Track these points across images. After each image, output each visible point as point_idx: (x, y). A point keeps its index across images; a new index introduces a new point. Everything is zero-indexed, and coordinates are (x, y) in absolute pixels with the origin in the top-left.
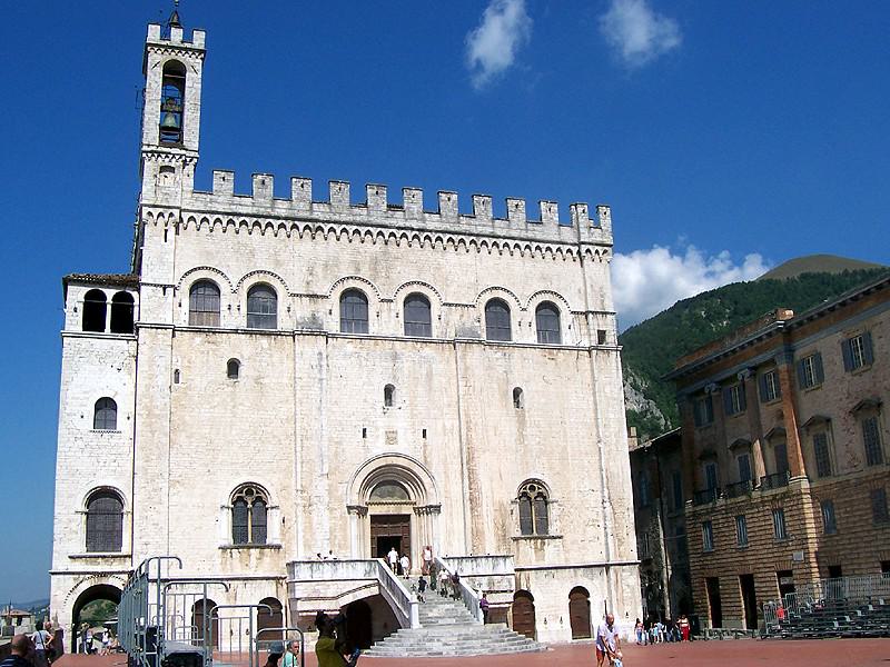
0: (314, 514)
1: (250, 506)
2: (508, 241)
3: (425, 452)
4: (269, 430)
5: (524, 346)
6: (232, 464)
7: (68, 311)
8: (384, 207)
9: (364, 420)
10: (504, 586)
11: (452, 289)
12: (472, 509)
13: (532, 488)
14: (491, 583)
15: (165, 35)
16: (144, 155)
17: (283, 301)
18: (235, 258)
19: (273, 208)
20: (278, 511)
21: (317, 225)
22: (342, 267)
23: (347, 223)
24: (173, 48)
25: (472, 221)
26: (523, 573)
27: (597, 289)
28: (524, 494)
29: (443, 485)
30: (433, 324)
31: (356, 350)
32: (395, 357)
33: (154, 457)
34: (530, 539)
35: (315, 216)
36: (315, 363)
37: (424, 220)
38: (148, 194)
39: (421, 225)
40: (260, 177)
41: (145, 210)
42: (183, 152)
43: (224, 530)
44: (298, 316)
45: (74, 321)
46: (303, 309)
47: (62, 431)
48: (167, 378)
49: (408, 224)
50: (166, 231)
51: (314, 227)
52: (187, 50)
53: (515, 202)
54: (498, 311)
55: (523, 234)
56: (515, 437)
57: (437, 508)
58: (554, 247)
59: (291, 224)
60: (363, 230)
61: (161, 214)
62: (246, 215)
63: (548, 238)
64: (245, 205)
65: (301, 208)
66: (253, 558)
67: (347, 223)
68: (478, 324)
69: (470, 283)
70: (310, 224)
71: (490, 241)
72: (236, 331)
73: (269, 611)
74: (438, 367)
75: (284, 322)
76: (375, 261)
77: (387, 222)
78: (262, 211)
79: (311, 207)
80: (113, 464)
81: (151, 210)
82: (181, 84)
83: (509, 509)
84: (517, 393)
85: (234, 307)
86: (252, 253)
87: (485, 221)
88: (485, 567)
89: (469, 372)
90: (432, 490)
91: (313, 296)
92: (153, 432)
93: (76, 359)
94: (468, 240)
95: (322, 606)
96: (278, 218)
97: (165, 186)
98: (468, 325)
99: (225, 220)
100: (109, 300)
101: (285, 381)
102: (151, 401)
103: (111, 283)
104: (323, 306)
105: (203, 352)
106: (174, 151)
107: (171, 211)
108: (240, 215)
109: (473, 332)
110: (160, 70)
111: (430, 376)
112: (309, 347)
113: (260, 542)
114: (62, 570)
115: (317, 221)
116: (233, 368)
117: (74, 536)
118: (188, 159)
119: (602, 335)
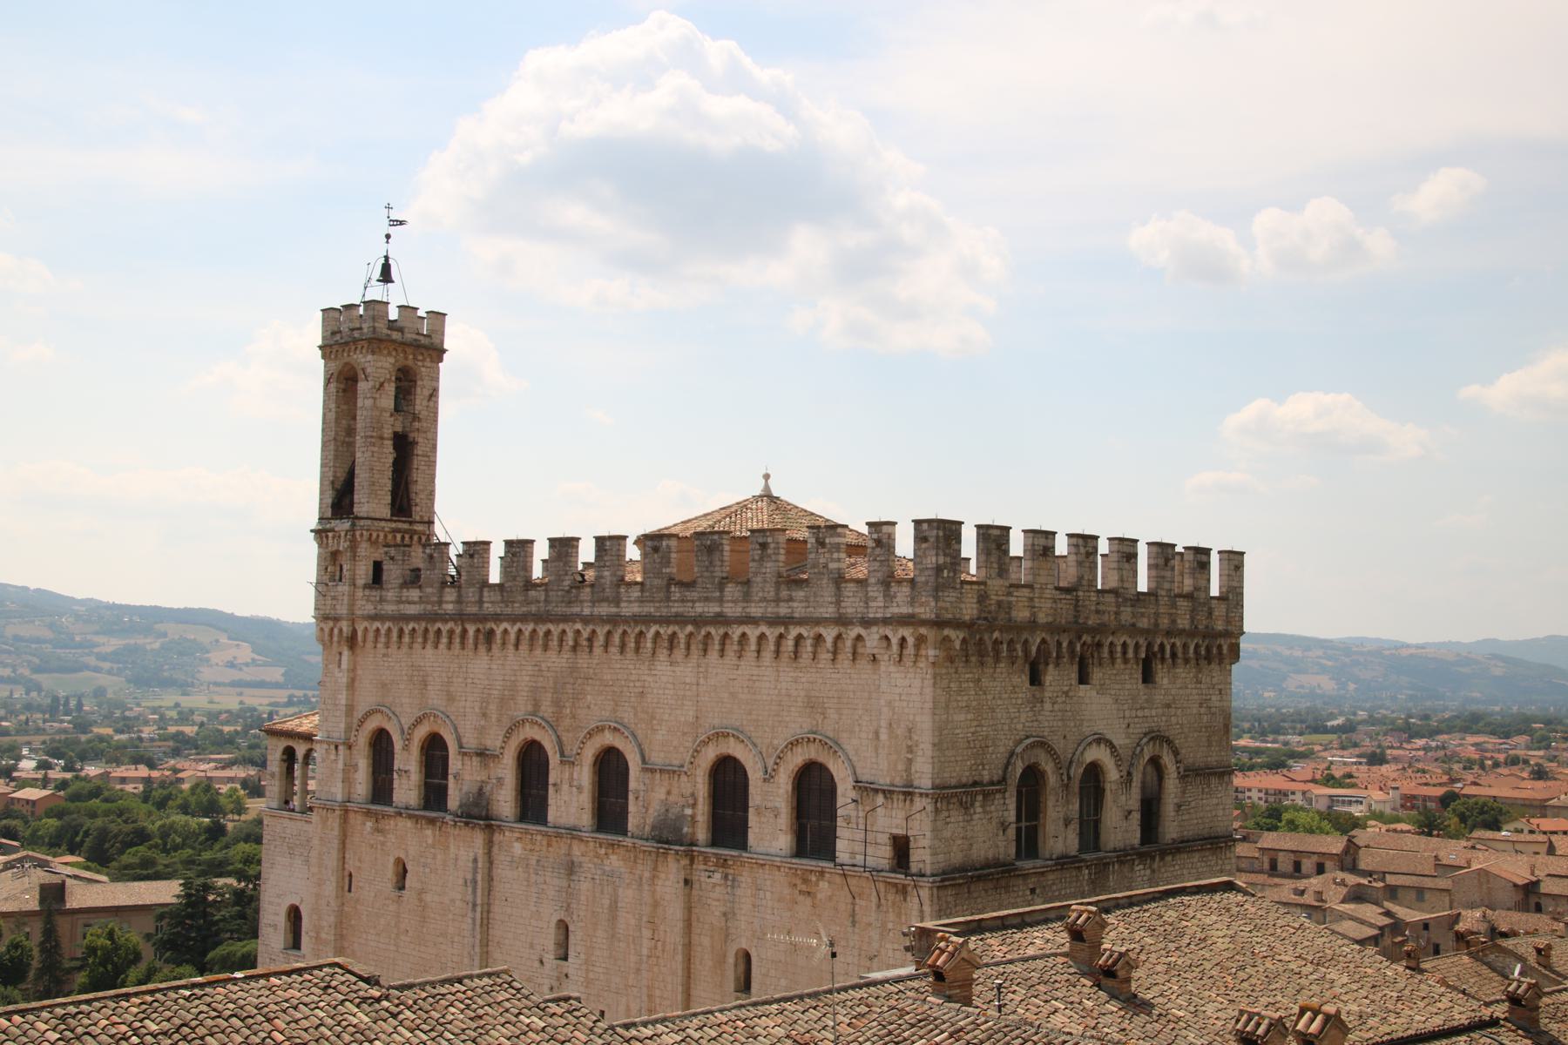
2: (748, 630)
11: (659, 737)
17: (454, 764)
19: (440, 603)
21: (489, 625)
32: (571, 869)
36: (469, 876)
37: (617, 601)
39: (614, 610)
44: (465, 789)
48: (330, 889)
49: (596, 611)
54: (728, 783)
55: (771, 610)
58: (829, 634)
62: (416, 618)
68: (688, 811)
71: (716, 632)
74: (627, 895)
77: (569, 611)
79: (481, 596)
86: (425, 684)
91: (483, 754)
111: (614, 907)
115: (482, 619)
116: (402, 873)
119: (901, 848)
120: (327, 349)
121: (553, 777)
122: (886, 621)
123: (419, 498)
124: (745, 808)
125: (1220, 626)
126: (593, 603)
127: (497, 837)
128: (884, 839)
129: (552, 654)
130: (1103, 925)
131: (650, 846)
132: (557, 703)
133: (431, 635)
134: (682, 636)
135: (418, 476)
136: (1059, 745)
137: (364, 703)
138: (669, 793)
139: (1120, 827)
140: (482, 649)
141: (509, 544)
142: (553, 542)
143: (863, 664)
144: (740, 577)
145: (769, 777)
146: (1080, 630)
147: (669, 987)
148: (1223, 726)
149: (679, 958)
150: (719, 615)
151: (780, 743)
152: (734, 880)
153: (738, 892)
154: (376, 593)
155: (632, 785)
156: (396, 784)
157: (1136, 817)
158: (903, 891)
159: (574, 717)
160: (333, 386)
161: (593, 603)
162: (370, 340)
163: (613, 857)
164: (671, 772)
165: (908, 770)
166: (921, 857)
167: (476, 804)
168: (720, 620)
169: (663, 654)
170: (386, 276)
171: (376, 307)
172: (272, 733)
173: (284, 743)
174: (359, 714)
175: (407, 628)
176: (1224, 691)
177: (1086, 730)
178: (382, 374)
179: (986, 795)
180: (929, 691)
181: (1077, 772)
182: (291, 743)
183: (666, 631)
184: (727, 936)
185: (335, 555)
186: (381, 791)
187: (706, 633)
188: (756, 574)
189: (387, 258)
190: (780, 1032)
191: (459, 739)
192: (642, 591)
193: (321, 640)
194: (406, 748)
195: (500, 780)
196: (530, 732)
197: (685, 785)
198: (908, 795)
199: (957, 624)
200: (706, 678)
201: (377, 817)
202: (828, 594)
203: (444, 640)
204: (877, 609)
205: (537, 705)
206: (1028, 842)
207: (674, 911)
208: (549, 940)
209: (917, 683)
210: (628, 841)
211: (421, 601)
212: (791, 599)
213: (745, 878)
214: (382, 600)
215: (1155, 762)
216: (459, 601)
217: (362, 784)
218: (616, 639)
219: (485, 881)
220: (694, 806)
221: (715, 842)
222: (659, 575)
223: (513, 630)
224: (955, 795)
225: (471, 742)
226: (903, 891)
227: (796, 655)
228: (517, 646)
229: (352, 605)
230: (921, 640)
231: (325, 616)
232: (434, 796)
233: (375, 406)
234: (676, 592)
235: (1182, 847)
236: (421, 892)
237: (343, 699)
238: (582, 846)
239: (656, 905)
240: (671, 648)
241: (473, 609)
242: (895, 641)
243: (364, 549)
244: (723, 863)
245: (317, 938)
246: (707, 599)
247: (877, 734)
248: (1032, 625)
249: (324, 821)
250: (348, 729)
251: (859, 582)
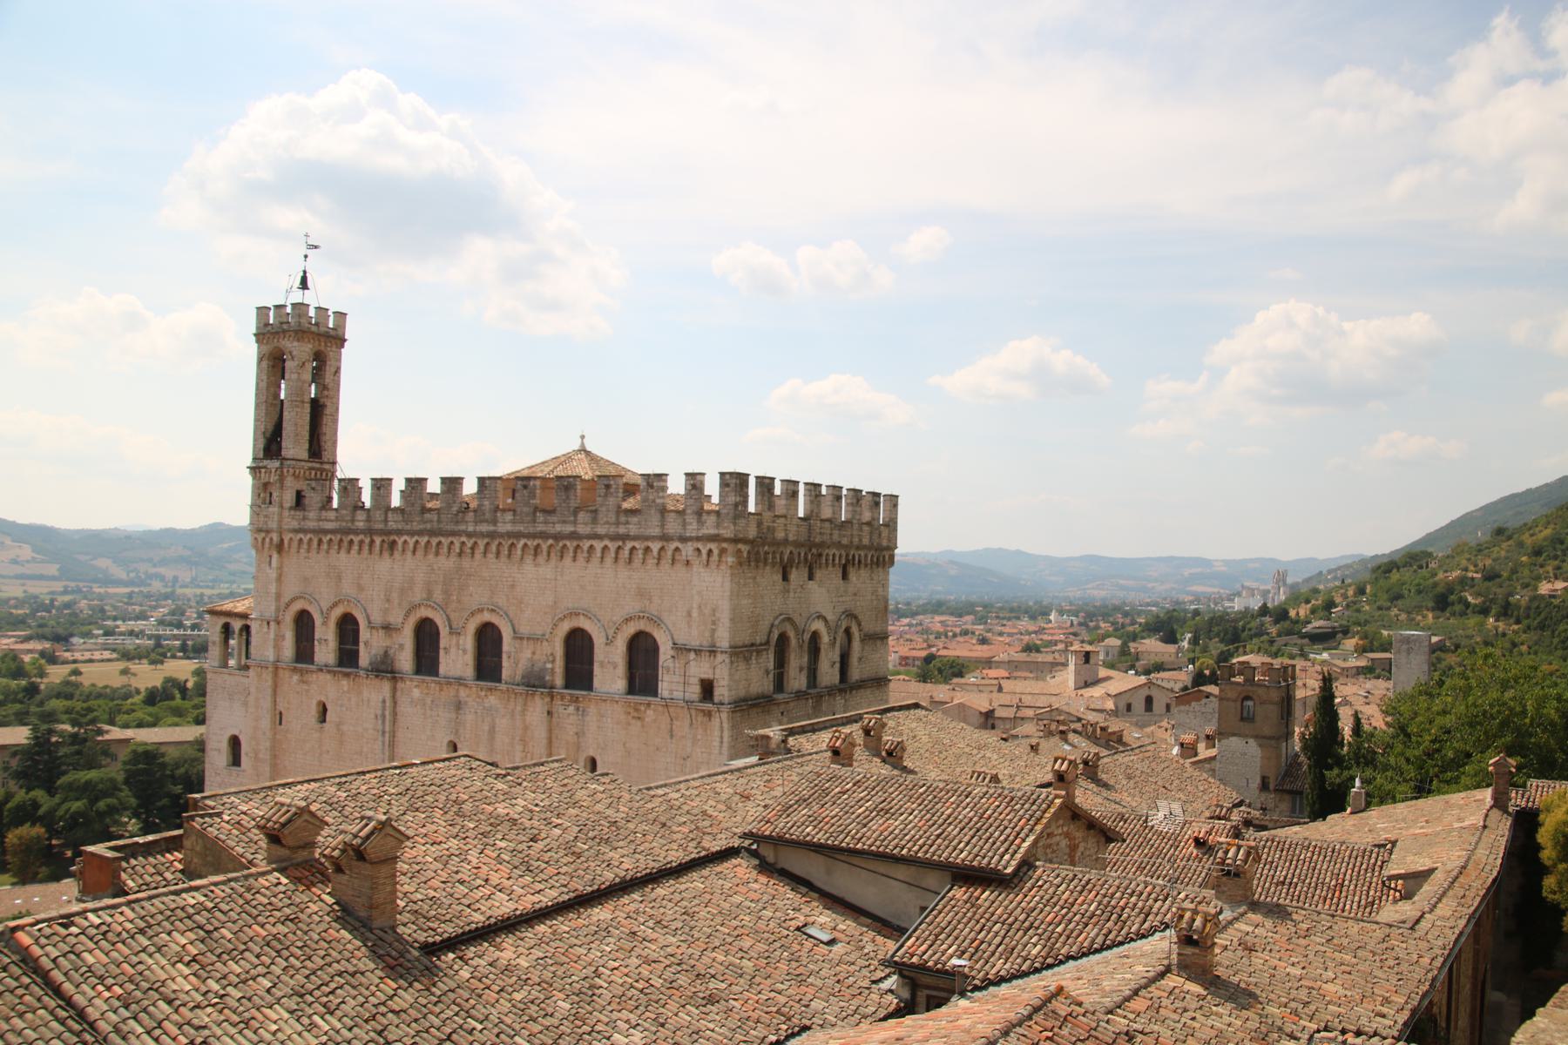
17: (364, 634)
19: (353, 521)
27: (707, 611)
32: (459, 706)
36: (379, 712)
39: (492, 528)
48: (266, 723)
55: (612, 530)
60: (434, 541)
71: (571, 544)
74: (502, 723)
75: (364, 659)
77: (456, 528)
86: (339, 578)
91: (387, 628)
96: (356, 532)
111: (492, 731)
112: (377, 692)
115: (390, 533)
116: (323, 710)
119: (707, 688)
120: (260, 336)
121: (442, 643)
122: (698, 539)
123: (327, 446)
124: (591, 663)
125: (885, 543)
126: (476, 523)
127: (400, 685)
128: (695, 681)
129: (442, 559)
130: (884, 725)
131: (520, 689)
132: (446, 592)
133: (345, 544)
134: (544, 547)
135: (325, 429)
136: (797, 619)
137: (291, 590)
139: (828, 673)
140: (386, 554)
141: (409, 481)
142: (409, 481)
143: (678, 566)
144: (566, 506)
145: (609, 642)
146: (811, 545)
148: (883, 609)
150: (574, 533)
151: (618, 618)
153: (588, 718)
154: (299, 514)
155: (505, 647)
156: (317, 649)
157: (838, 665)
158: (709, 714)
159: (459, 601)
160: (265, 364)
161: (476, 523)
162: (296, 332)
163: (492, 698)
164: (534, 639)
165: (712, 636)
166: (722, 692)
167: (383, 662)
168: (574, 536)
169: (529, 559)
170: (304, 284)
171: (300, 307)
172: (212, 612)
173: (223, 620)
174: (286, 598)
175: (326, 539)
176: (885, 586)
177: (812, 610)
178: (299, 356)
179: (758, 652)
180: (727, 585)
181: (807, 637)
182: (228, 620)
183: (532, 543)
185: (266, 485)
186: (304, 652)
187: (563, 544)
190: (730, 790)
191: (368, 617)
193: (255, 547)
194: (325, 623)
195: (401, 646)
196: (424, 613)
197: (546, 648)
198: (713, 652)
199: (744, 541)
201: (301, 672)
202: (655, 519)
203: (356, 547)
204: (692, 529)
205: (430, 593)
206: (779, 685)
207: (540, 733)
209: (719, 579)
210: (503, 687)
211: (337, 519)
213: (592, 709)
214: (304, 518)
215: (848, 631)
216: (368, 520)
217: (288, 649)
218: (494, 547)
219: (391, 716)
220: (553, 661)
221: (567, 687)
222: (527, 504)
223: (411, 541)
224: (742, 652)
225: (377, 618)
226: (709, 714)
227: (630, 560)
228: (414, 552)
229: (280, 521)
230: (723, 552)
231: (259, 528)
232: (348, 657)
233: (299, 379)
234: (540, 517)
235: (862, 685)
236: (338, 725)
237: (273, 589)
239: (526, 728)
240: (536, 555)
241: (381, 526)
242: (704, 552)
243: (289, 481)
244: (576, 700)
245: (256, 758)
246: (564, 522)
247: (689, 614)
248: (786, 542)
249: (259, 676)
250: (278, 610)
251: (678, 512)
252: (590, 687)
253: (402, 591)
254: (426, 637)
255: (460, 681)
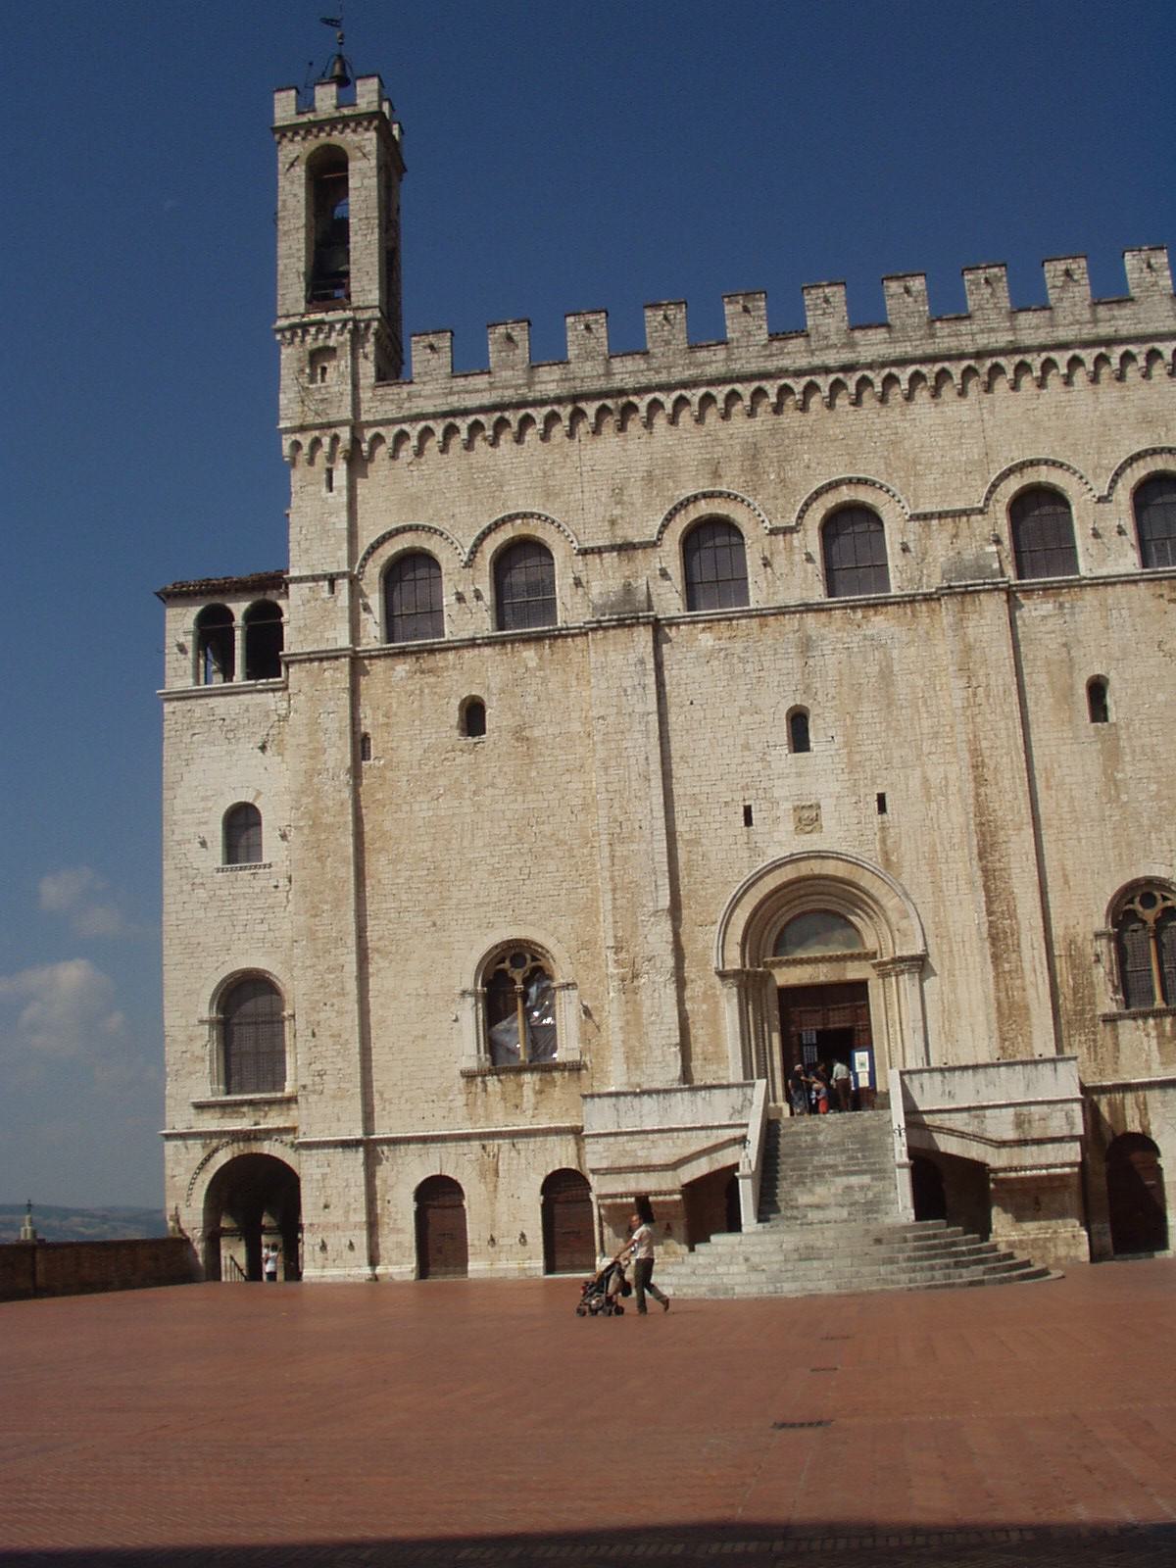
0: (644, 996)
1: (519, 986)
2: (1054, 355)
3: (883, 841)
4: (547, 829)
5: (1107, 582)
6: (481, 905)
7: (172, 655)
8: (763, 336)
9: (746, 788)
10: (1057, 1125)
11: (929, 481)
12: (996, 958)
13: (1148, 901)
14: (1019, 1124)
15: (305, 104)
16: (278, 337)
17: (564, 568)
18: (450, 501)
19: (530, 384)
20: (574, 993)
21: (624, 400)
22: (684, 477)
23: (685, 385)
24: (320, 125)
25: (964, 327)
26: (1130, 1098)
28: (1132, 915)
29: (929, 905)
30: (890, 564)
31: (723, 644)
32: (806, 646)
33: (326, 907)
34: (1145, 1016)
35: (616, 383)
37: (851, 345)
38: (290, 407)
39: (846, 356)
40: (501, 330)
41: (286, 442)
42: (349, 314)
43: (462, 1037)
44: (596, 589)
45: (180, 670)
46: (605, 580)
47: (169, 874)
48: (340, 753)
49: (817, 361)
50: (330, 471)
51: (619, 409)
52: (345, 121)
53: (1061, 266)
55: (1087, 332)
56: (1096, 787)
57: (920, 965)
59: (570, 408)
60: (720, 392)
61: (316, 443)
63: (1150, 329)
64: (477, 391)
65: (587, 372)
66: (528, 1092)
67: (685, 385)
68: (993, 548)
69: (969, 462)
70: (609, 403)
71: (1008, 363)
72: (472, 643)
73: (564, 1192)
75: (570, 609)
76: (753, 453)
77: (771, 365)
78: (509, 395)
80: (258, 927)
81: (298, 437)
82: (341, 187)
83: (1089, 951)
84: (1097, 690)
85: (469, 595)
87: (996, 319)
88: (1011, 1086)
89: (976, 655)
90: (904, 924)
91: (625, 548)
92: (319, 859)
93: (187, 739)
94: (956, 369)
95: (647, 1183)
97: (314, 391)
98: (969, 555)
99: (439, 428)
100: (239, 621)
101: (576, 727)
102: (316, 802)
103: (239, 588)
104: (646, 567)
105: (412, 693)
106: (330, 316)
107: (334, 431)
108: (465, 412)
109: (980, 570)
110: (300, 171)
111: (886, 675)
113: (540, 1056)
114: (181, 1128)
115: (622, 392)
116: (473, 717)
117: (198, 1067)
118: (362, 325)
126: (812, 353)
129: (738, 422)
138: (956, 536)
147: (1003, 733)
149: (1016, 699)
152: (1072, 607)
169: (922, 395)
174: (365, 541)
183: (929, 370)
184: (1071, 667)
188: (1061, 300)
189: (340, 57)
192: (889, 332)
194: (469, 564)
195: (664, 574)
200: (992, 412)
205: (716, 475)
208: (781, 733)
211: (492, 386)
212: (1113, 318)
214: (410, 397)
223: (668, 400)
237: (341, 522)
238: (823, 616)
239: (968, 649)
246: (992, 330)
252: (1075, 569)
253: (649, 478)
254: (710, 549)
255: (808, 608)
